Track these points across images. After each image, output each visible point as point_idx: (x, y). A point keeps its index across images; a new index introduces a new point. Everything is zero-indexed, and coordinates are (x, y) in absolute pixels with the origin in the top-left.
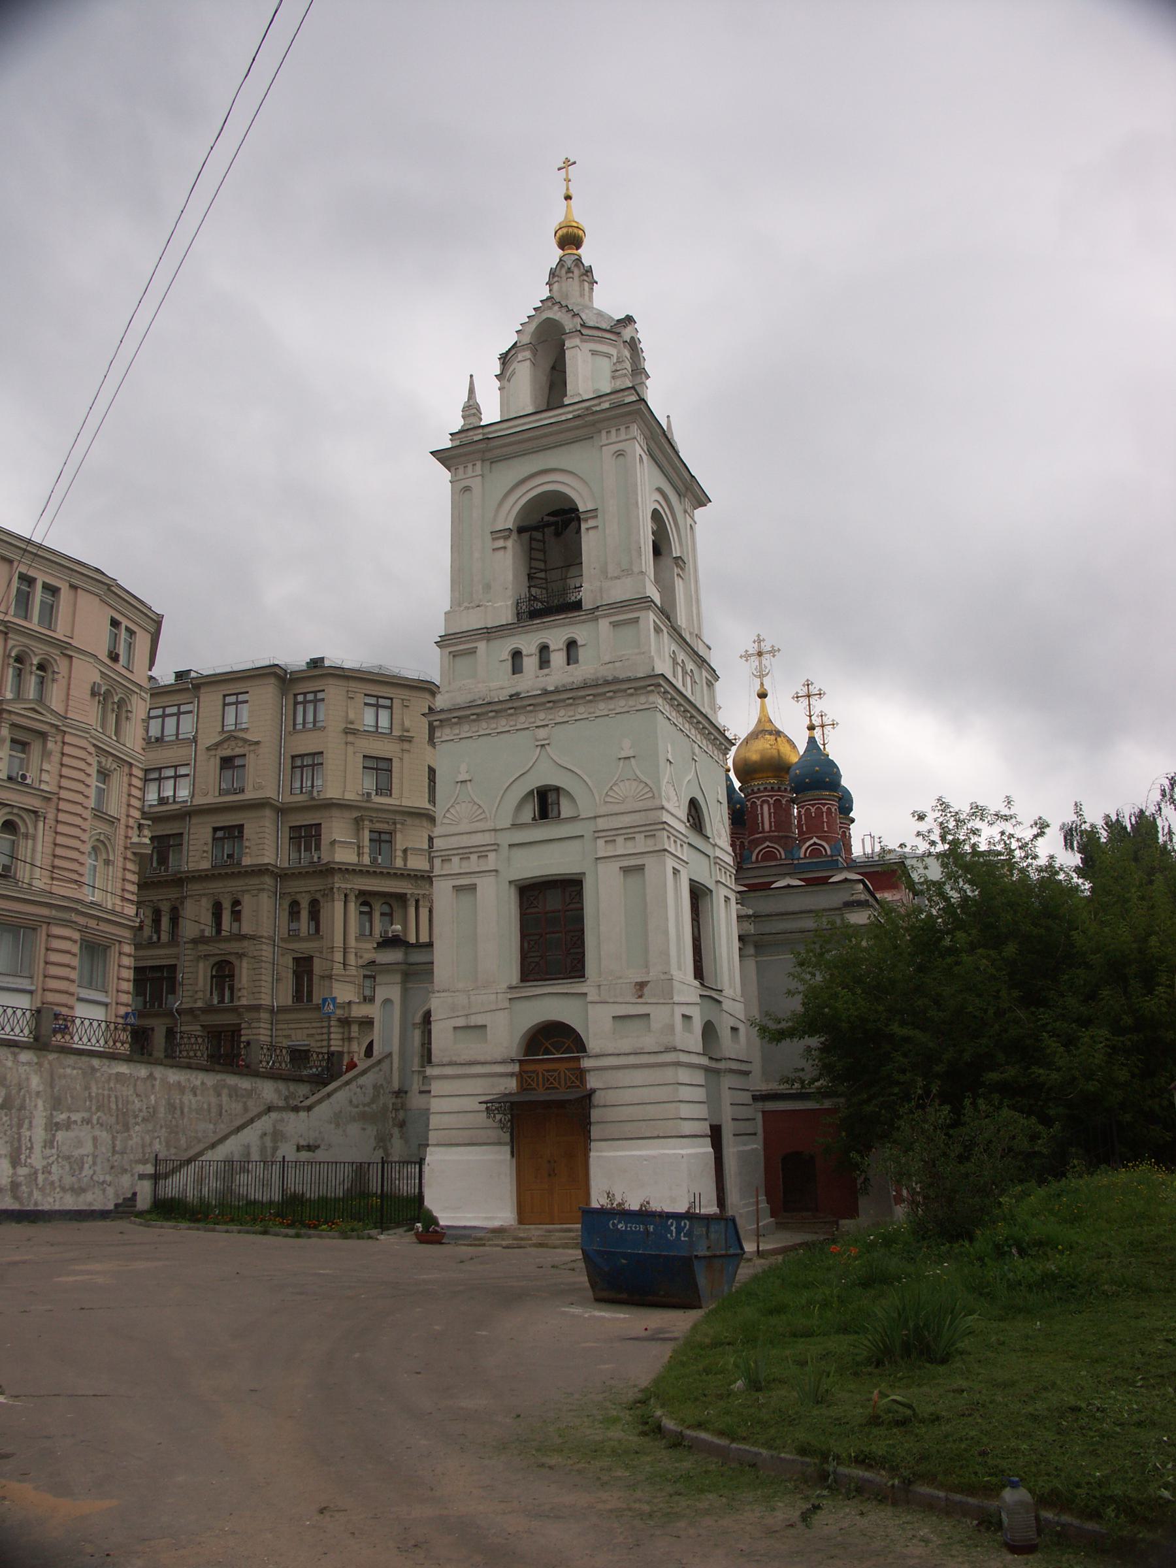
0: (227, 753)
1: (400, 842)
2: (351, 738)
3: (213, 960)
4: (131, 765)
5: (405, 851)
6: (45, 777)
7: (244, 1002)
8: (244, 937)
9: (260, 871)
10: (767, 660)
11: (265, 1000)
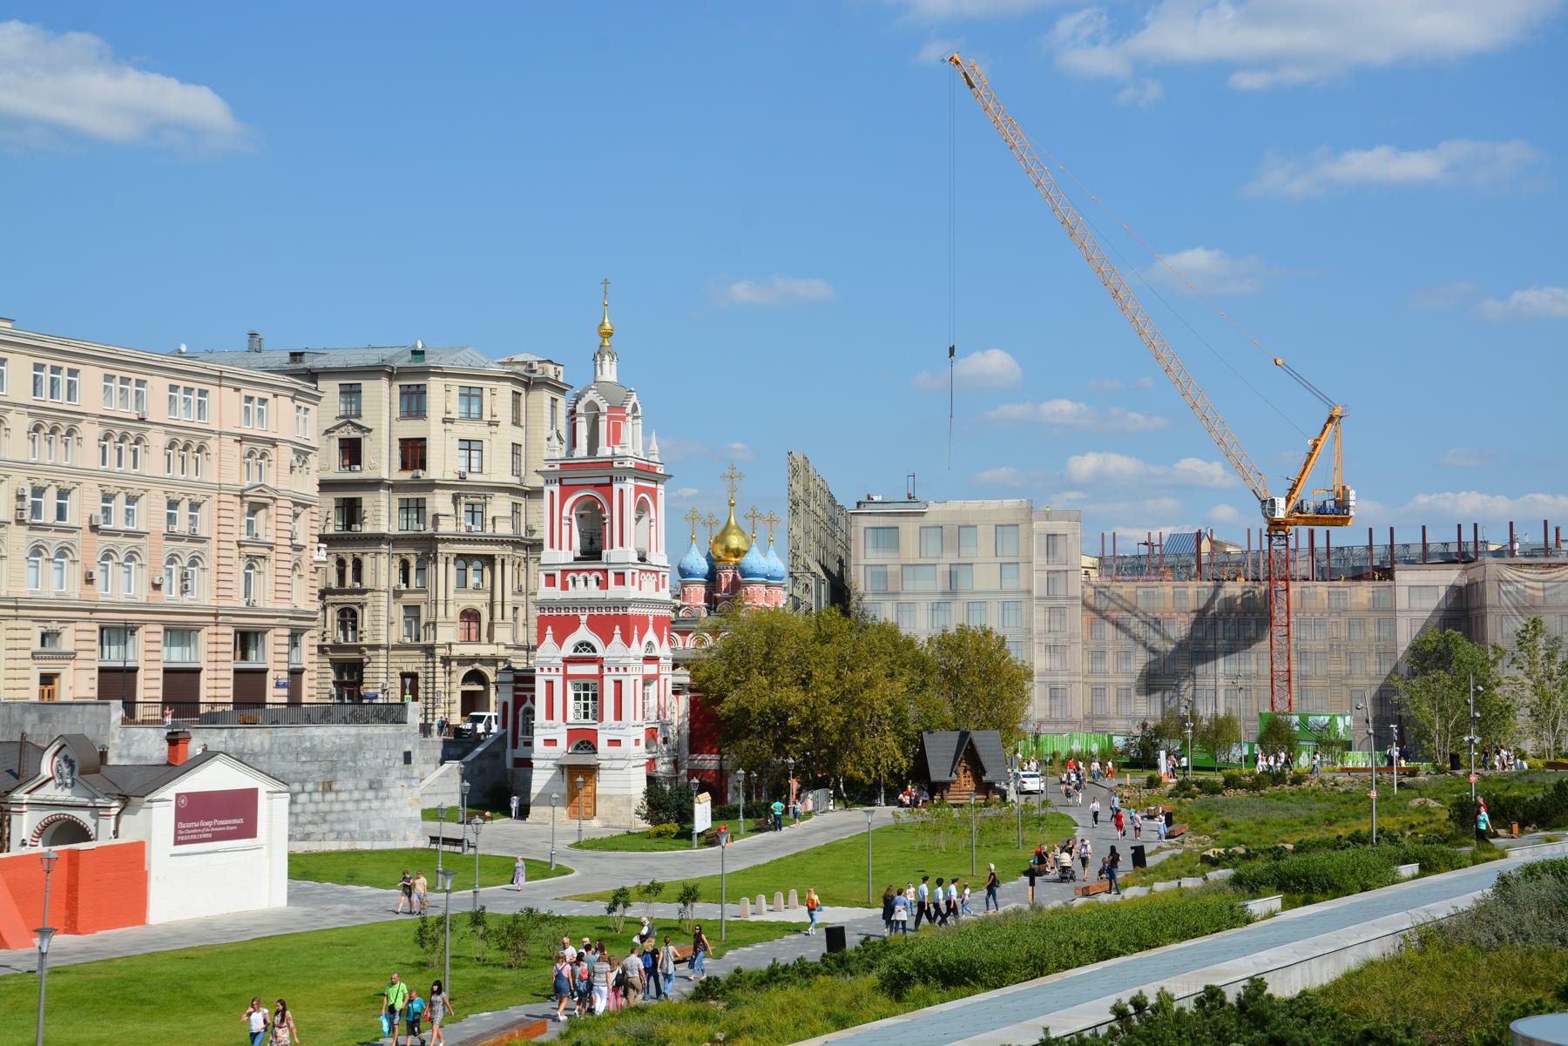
0: (345, 435)
1: (490, 512)
2: (449, 426)
3: (338, 607)
4: (310, 506)
5: (494, 519)
6: (269, 532)
7: (366, 642)
8: (364, 592)
9: (377, 539)
10: (737, 482)
11: (383, 641)
